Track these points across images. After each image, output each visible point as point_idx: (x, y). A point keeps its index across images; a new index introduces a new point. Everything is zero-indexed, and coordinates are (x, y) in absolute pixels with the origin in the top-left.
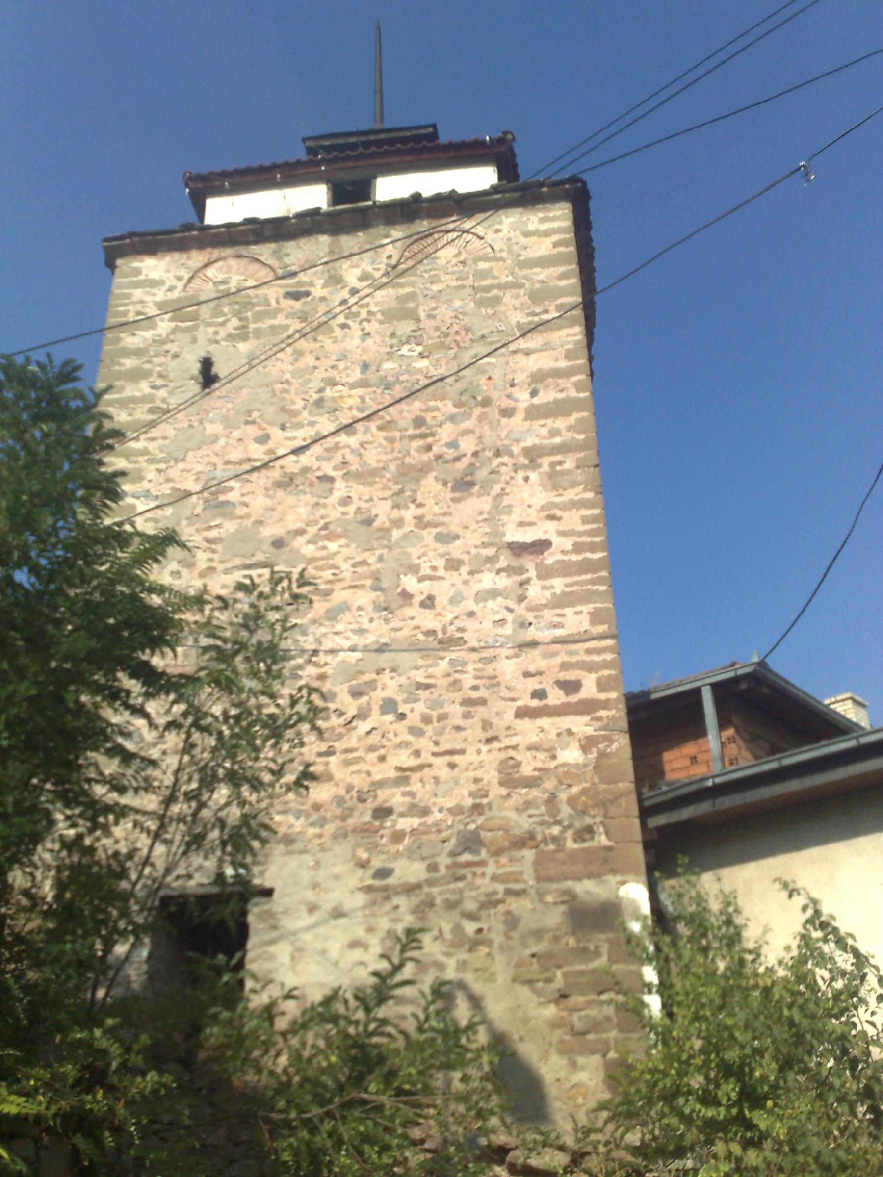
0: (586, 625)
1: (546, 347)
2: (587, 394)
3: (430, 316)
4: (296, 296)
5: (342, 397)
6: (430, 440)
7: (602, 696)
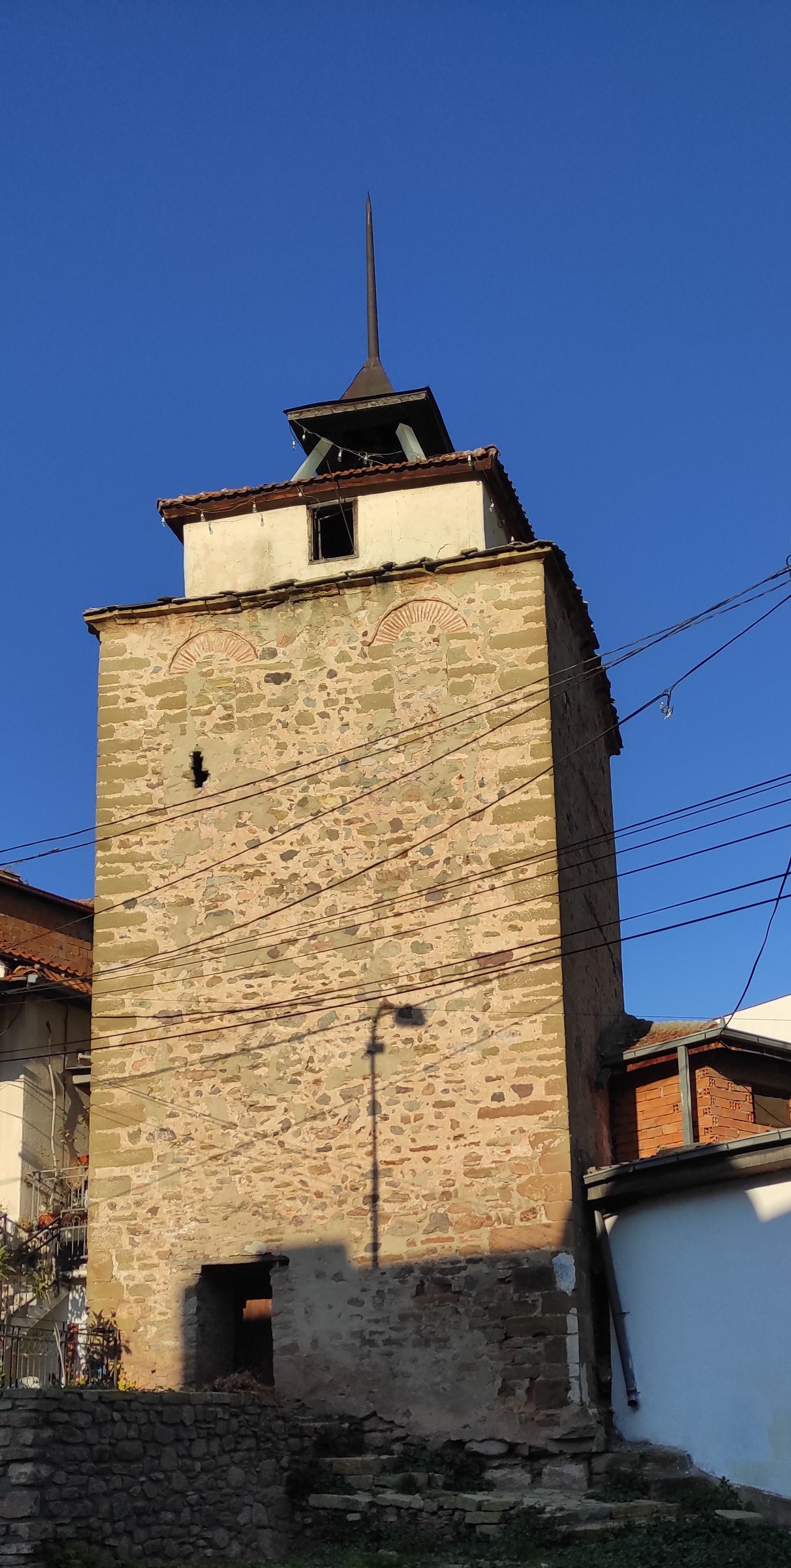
0: (539, 1034)
1: (515, 742)
2: (550, 796)
3: (406, 705)
4: (277, 679)
5: (324, 797)
6: (407, 845)
7: (550, 1098)
